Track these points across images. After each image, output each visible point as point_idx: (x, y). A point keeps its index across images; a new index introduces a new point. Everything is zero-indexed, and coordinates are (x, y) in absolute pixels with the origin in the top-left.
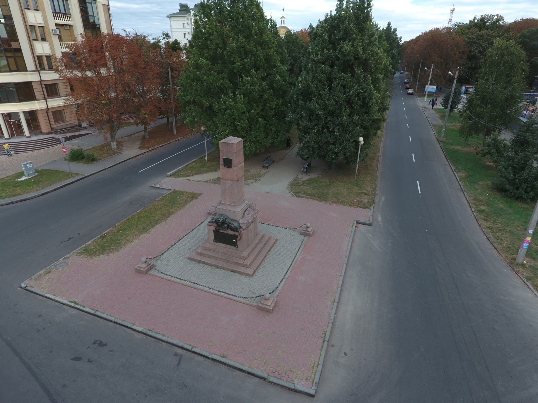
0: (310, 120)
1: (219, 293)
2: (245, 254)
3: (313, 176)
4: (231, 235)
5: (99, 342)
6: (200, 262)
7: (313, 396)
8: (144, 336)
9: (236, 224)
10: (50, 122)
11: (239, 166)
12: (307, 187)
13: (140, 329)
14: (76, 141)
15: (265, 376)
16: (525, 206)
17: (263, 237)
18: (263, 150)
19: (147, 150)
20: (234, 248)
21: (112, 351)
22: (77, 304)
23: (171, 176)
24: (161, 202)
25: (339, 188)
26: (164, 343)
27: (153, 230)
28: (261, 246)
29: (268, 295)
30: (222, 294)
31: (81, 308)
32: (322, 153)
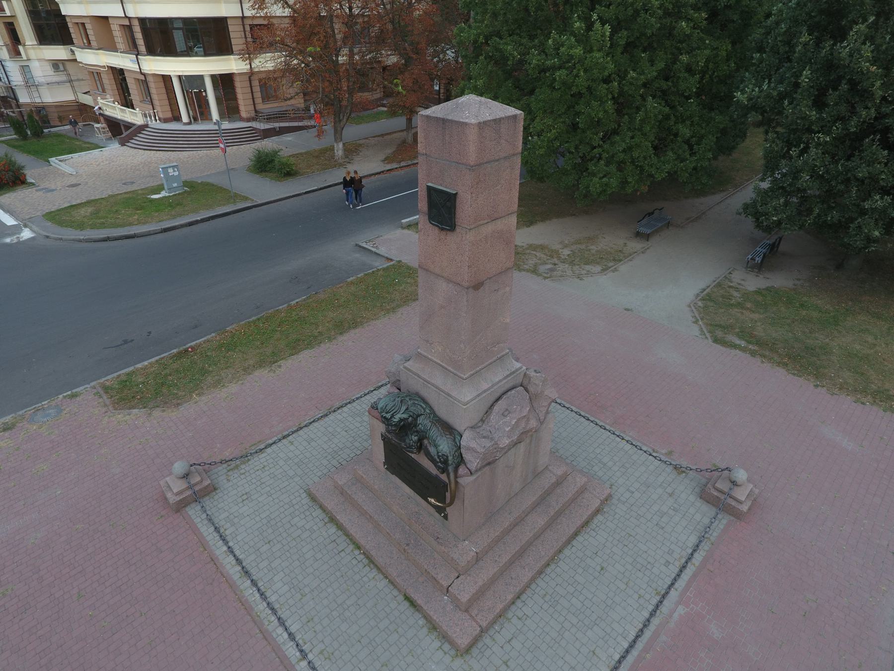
2: (467, 550)
3: (779, 281)
6: (333, 520)
10: (253, 99)
11: (489, 229)
12: (756, 316)
14: (288, 138)
17: (558, 483)
18: (644, 189)
19: (394, 166)
20: (437, 514)
23: (409, 226)
24: (353, 288)
25: (870, 339)
27: (288, 364)
28: (539, 520)
32: (834, 216)
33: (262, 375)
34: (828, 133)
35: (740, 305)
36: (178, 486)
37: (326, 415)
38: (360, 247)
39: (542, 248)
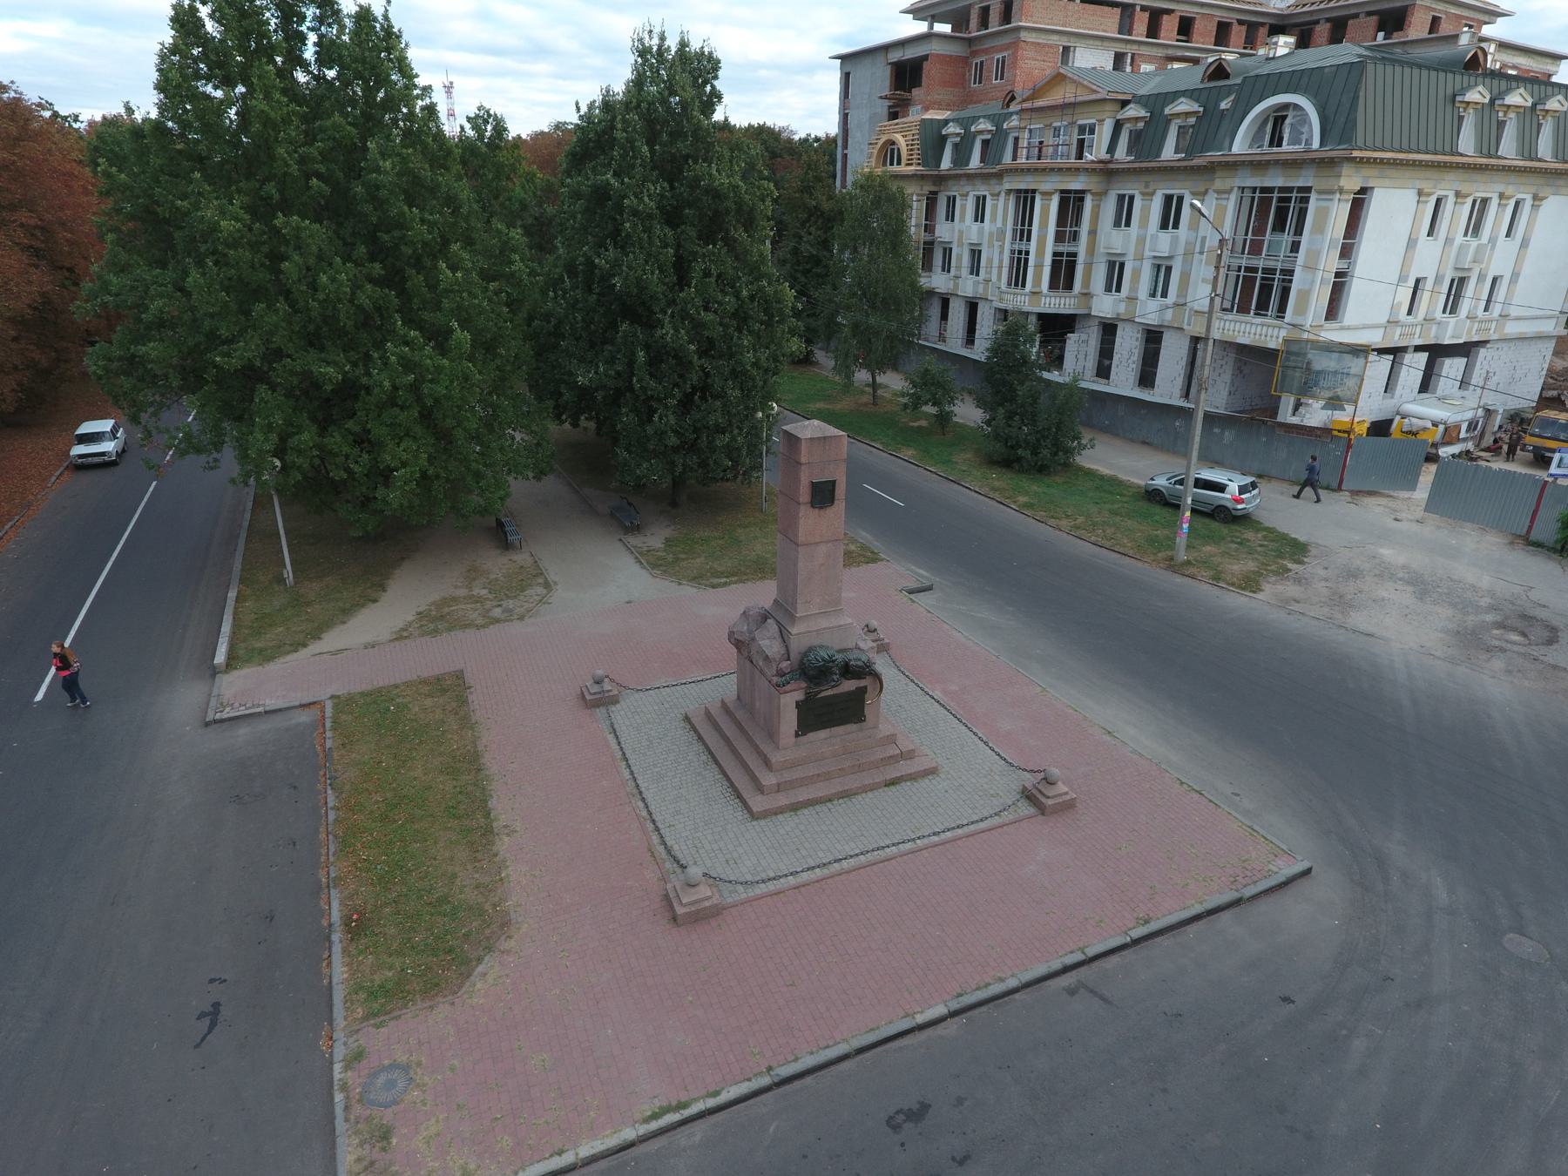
0: (651, 375)
1: (943, 836)
2: (885, 729)
4: (849, 693)
5: (901, 1117)
6: (795, 808)
7: (1307, 872)
8: (963, 1019)
9: (864, 658)
13: (940, 1010)
15: (1236, 895)
16: (1059, 479)
21: (960, 1101)
22: (684, 1106)
26: (1017, 996)
29: (1055, 771)
30: (949, 834)
31: (711, 1103)
33: (503, 845)
34: (674, 397)
35: (677, 560)
36: (704, 891)
37: (643, 800)
38: (222, 721)
39: (454, 599)
